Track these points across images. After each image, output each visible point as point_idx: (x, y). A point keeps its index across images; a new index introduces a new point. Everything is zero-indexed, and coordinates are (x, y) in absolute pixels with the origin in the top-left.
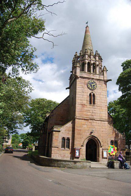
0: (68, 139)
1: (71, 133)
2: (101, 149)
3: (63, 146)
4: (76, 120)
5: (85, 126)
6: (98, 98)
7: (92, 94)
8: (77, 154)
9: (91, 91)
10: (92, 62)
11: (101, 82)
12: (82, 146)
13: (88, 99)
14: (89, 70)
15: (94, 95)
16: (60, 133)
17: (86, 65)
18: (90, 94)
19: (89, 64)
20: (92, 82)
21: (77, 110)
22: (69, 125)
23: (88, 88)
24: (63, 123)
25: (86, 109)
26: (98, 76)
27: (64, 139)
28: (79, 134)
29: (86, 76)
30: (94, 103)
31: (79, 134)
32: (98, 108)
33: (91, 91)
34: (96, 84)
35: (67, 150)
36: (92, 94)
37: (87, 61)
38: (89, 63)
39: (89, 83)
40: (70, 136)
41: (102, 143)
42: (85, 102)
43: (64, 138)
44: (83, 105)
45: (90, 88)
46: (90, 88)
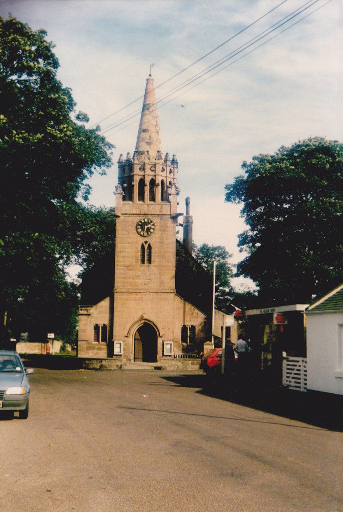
0: (104, 327)
1: (107, 316)
2: (160, 341)
3: (97, 339)
7: (146, 246)
9: (142, 240)
12: (127, 337)
20: (146, 220)
22: (105, 303)
24: (92, 300)
30: (150, 262)
33: (142, 240)
34: (153, 225)
36: (146, 246)
38: (142, 183)
39: (139, 225)
40: (107, 322)
43: (97, 325)
45: (142, 233)
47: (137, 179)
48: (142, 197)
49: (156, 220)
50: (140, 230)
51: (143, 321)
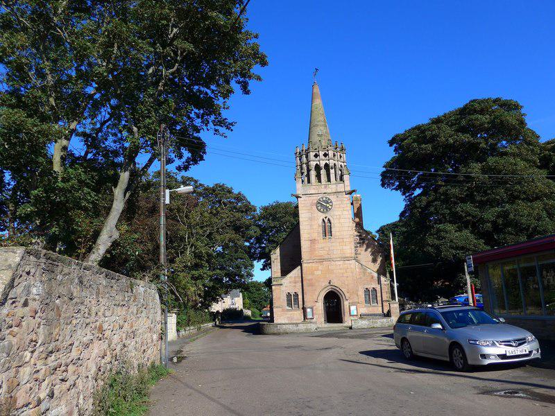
3: (289, 304)
4: (304, 265)
5: (319, 273)
6: (337, 225)
7: (326, 220)
8: (309, 316)
9: (324, 216)
10: (322, 164)
11: (340, 195)
13: (321, 230)
14: (318, 177)
15: (329, 219)
16: (283, 288)
17: (313, 173)
18: (323, 220)
19: (318, 168)
21: (303, 250)
22: (296, 272)
23: (319, 211)
25: (318, 246)
26: (334, 186)
27: (289, 295)
28: (312, 285)
29: (313, 192)
31: (312, 285)
32: (338, 241)
33: (322, 216)
35: (295, 310)
37: (313, 164)
38: (318, 168)
41: (347, 295)
42: (315, 236)
44: (313, 241)
46: (322, 210)
47: (313, 164)
48: (318, 177)
49: (333, 198)
50: (319, 208)
51: (330, 287)
